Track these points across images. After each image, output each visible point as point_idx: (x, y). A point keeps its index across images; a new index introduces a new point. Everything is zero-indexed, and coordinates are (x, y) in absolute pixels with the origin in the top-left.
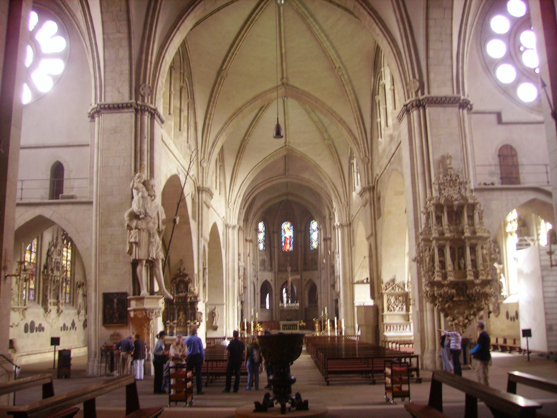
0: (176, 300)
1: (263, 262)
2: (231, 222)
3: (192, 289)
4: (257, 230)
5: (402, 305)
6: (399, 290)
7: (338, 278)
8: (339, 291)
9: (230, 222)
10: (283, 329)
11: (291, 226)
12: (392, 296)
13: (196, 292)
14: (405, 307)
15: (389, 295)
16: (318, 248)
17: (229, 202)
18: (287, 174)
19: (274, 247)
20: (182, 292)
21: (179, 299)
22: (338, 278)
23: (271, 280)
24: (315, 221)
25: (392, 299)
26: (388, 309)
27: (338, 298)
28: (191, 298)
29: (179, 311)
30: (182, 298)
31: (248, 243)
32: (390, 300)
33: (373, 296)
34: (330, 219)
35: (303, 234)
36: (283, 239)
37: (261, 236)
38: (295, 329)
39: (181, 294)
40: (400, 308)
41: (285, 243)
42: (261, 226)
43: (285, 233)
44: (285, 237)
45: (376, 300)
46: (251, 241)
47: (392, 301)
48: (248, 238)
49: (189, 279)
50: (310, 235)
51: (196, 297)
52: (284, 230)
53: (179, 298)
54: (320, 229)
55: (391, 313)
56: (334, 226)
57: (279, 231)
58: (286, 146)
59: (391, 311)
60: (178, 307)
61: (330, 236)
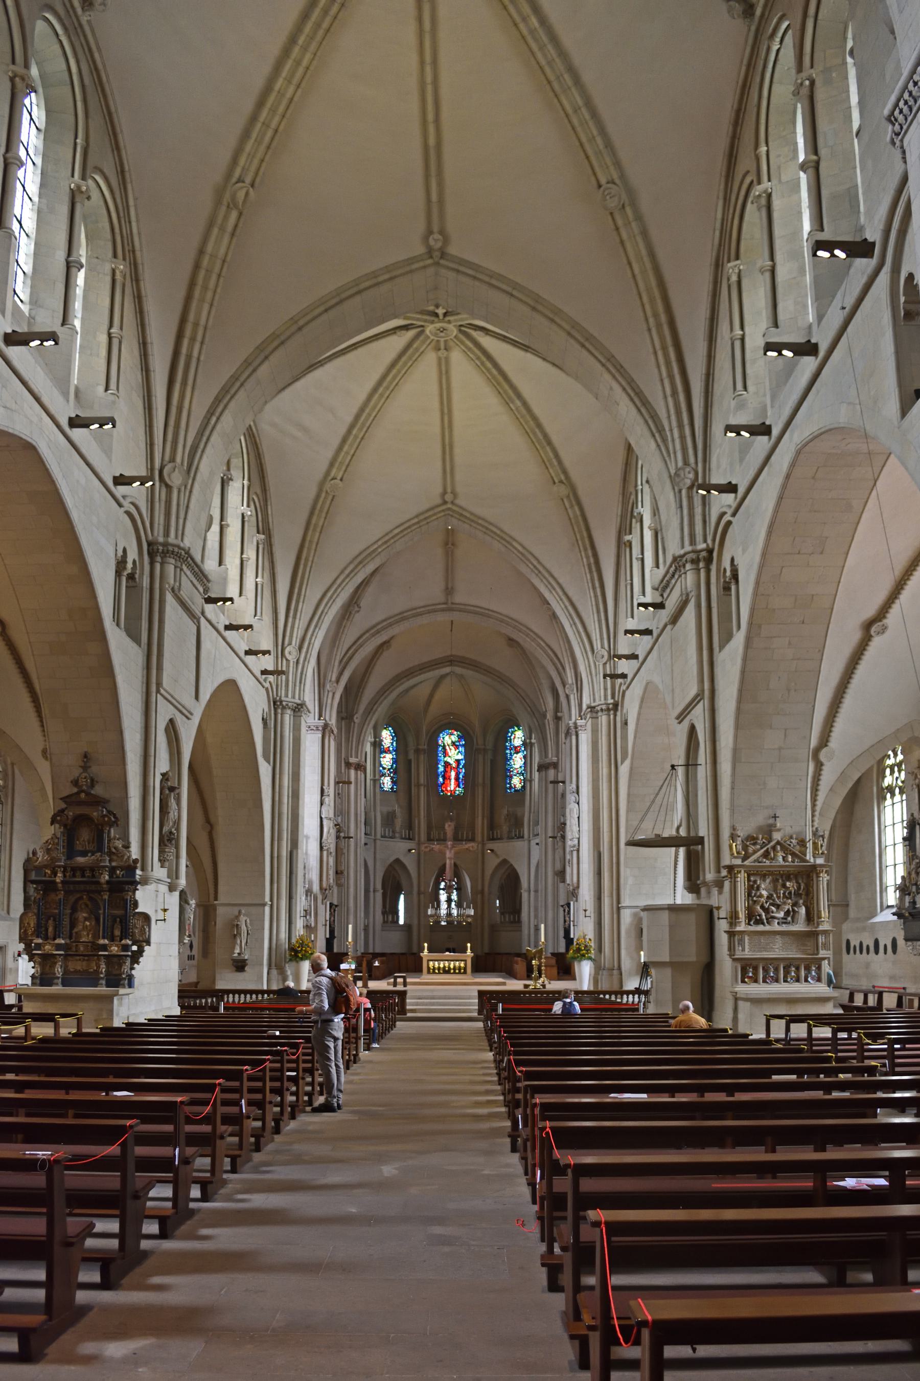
0: (65, 876)
1: (389, 819)
2: (290, 695)
3: (119, 844)
4: (377, 745)
5: (795, 904)
6: (784, 858)
9: (287, 696)
11: (460, 738)
12: (764, 877)
13: (135, 852)
14: (803, 910)
15: (754, 874)
16: (523, 787)
17: (286, 642)
18: (450, 602)
19: (418, 785)
20: (84, 854)
21: (74, 876)
24: (519, 729)
25: (763, 886)
26: (751, 917)
28: (112, 870)
29: (74, 910)
30: (82, 869)
31: (352, 772)
32: (758, 888)
33: (693, 885)
34: (558, 719)
35: (489, 756)
36: (441, 769)
37: (387, 760)
39: (80, 860)
40: (787, 913)
41: (446, 777)
42: (387, 737)
43: (445, 754)
44: (447, 764)
45: (703, 890)
47: (765, 893)
48: (353, 760)
49: (109, 812)
50: (506, 759)
51: (130, 869)
52: (444, 747)
53: (74, 870)
54: (532, 745)
55: (760, 928)
56: (568, 729)
57: (433, 749)
58: (445, 502)
59: (759, 922)
60: (72, 899)
61: (555, 759)
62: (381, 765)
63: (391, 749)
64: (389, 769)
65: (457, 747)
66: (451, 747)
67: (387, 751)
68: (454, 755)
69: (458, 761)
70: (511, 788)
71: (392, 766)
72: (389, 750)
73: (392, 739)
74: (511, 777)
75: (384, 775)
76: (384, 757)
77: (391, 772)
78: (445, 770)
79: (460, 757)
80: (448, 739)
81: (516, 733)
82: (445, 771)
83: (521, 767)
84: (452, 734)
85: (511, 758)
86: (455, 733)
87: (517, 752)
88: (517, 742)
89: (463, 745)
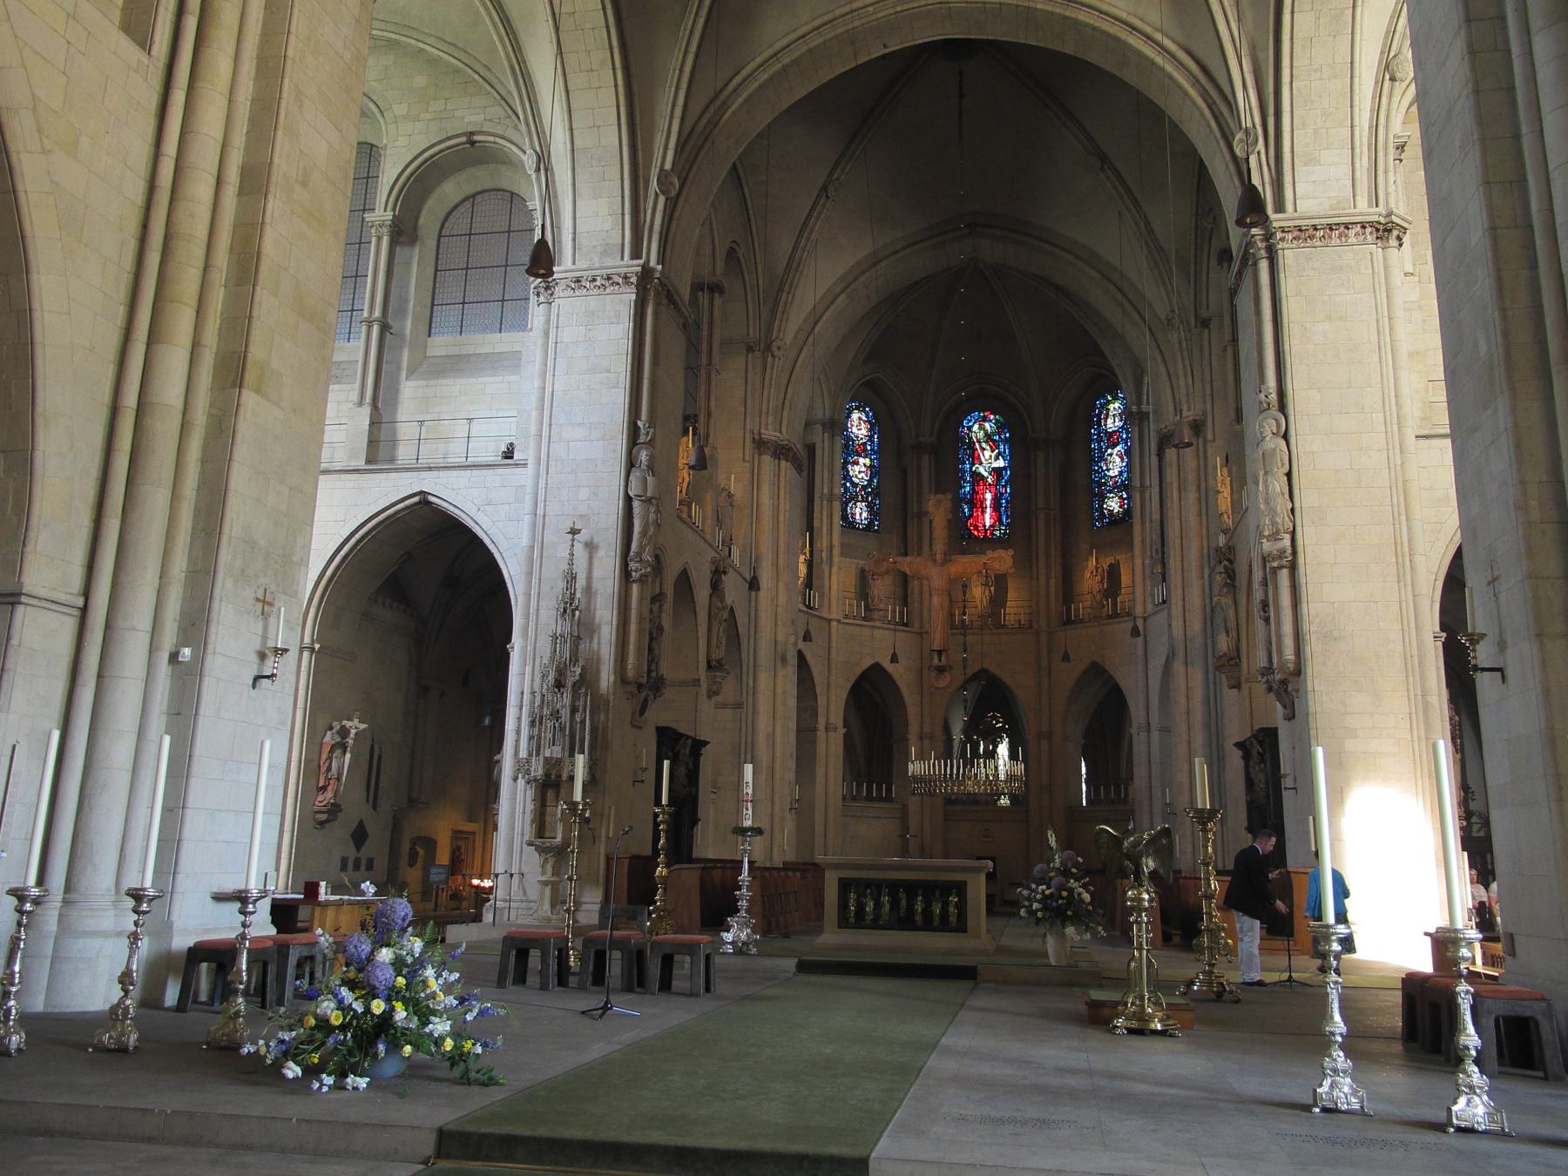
7: (1284, 575)
8: (1291, 666)
10: (843, 923)
11: (1000, 427)
22: (1284, 575)
23: (894, 659)
27: (1275, 714)
31: (767, 458)
38: (944, 926)
41: (976, 503)
43: (975, 459)
44: (977, 478)
46: (781, 452)
48: (770, 434)
62: (847, 477)
63: (869, 448)
64: (864, 488)
65: (995, 447)
66: (984, 445)
67: (862, 451)
68: (989, 461)
69: (997, 472)
70: (1102, 516)
71: (870, 481)
72: (865, 450)
73: (870, 430)
74: (1102, 498)
75: (854, 499)
76: (857, 464)
77: (868, 494)
78: (973, 489)
79: (1001, 463)
80: (979, 428)
81: (1111, 407)
82: (974, 492)
83: (1121, 473)
84: (985, 419)
85: (1102, 458)
86: (992, 417)
87: (1114, 445)
88: (1113, 424)
89: (1005, 441)
